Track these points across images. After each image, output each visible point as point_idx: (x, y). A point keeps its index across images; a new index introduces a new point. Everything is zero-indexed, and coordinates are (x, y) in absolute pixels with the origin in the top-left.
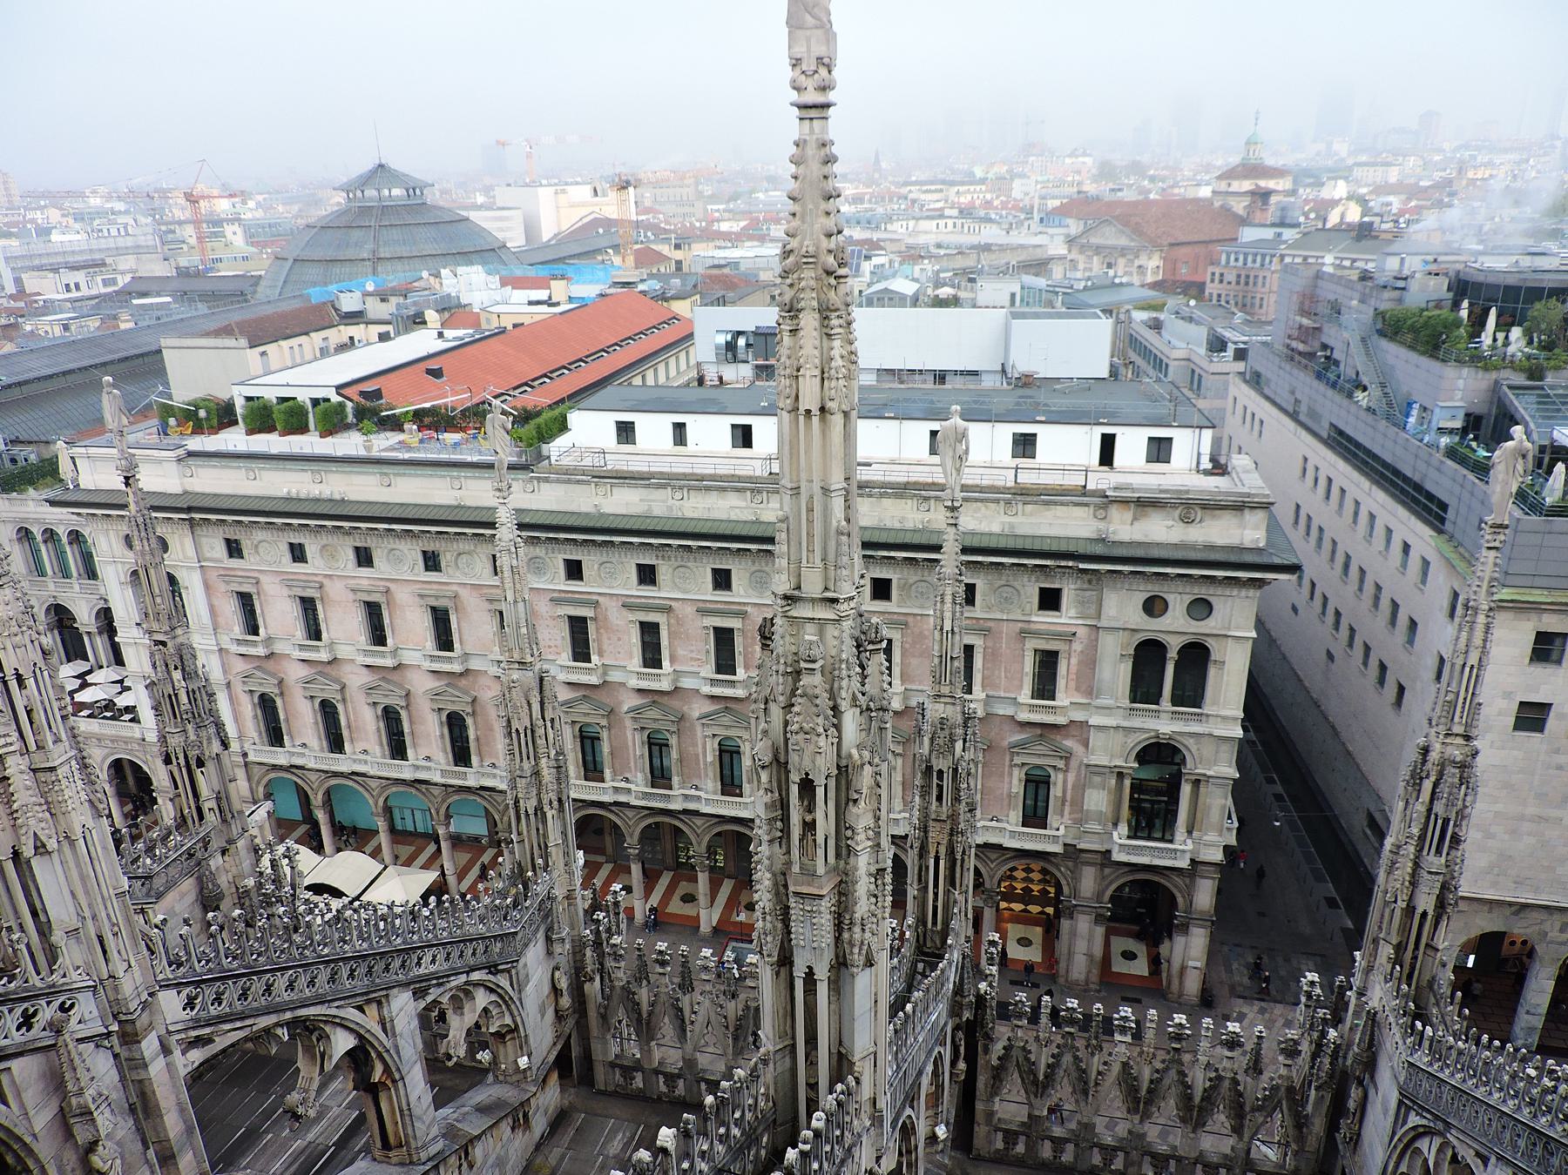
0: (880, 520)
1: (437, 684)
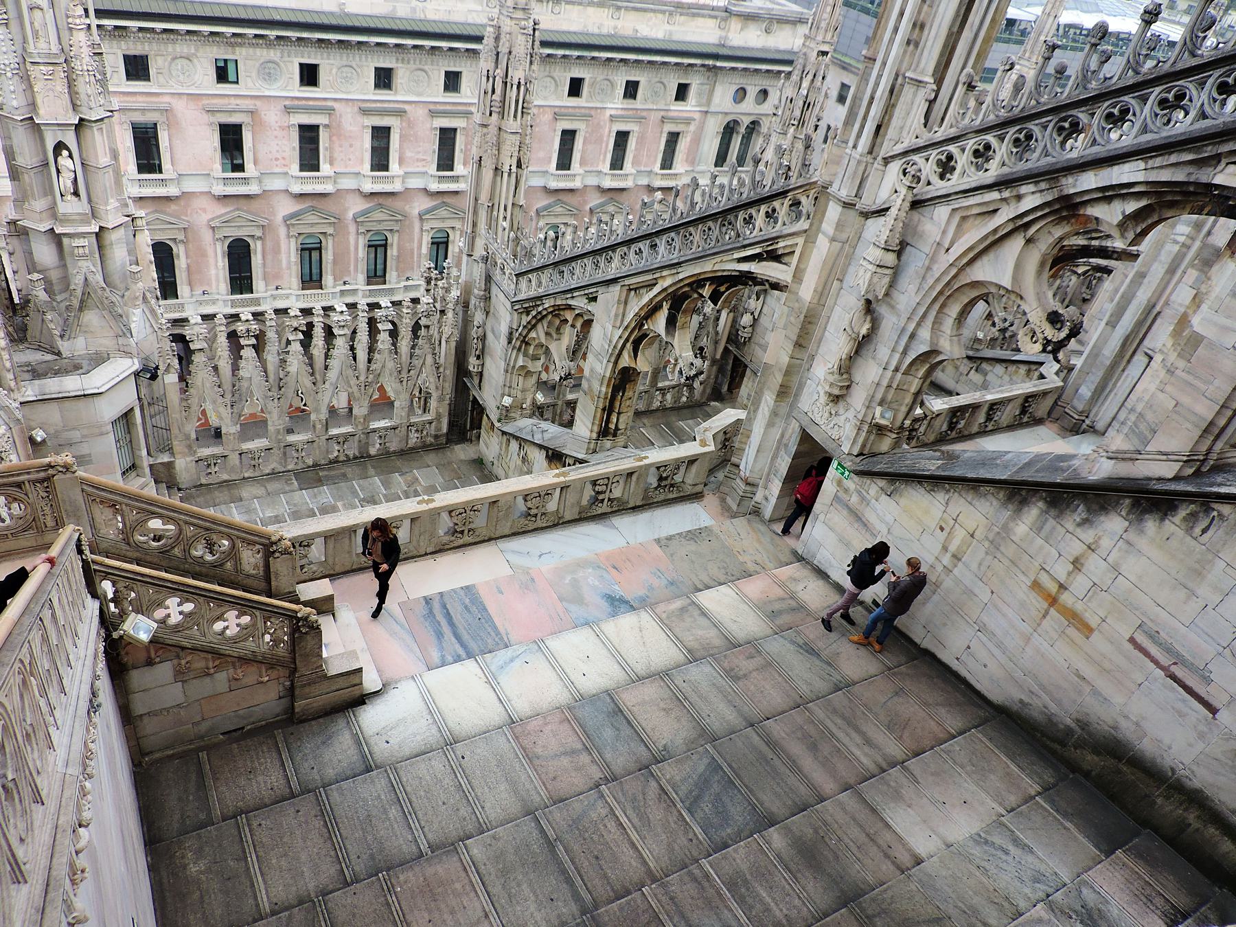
1: (223, 211)
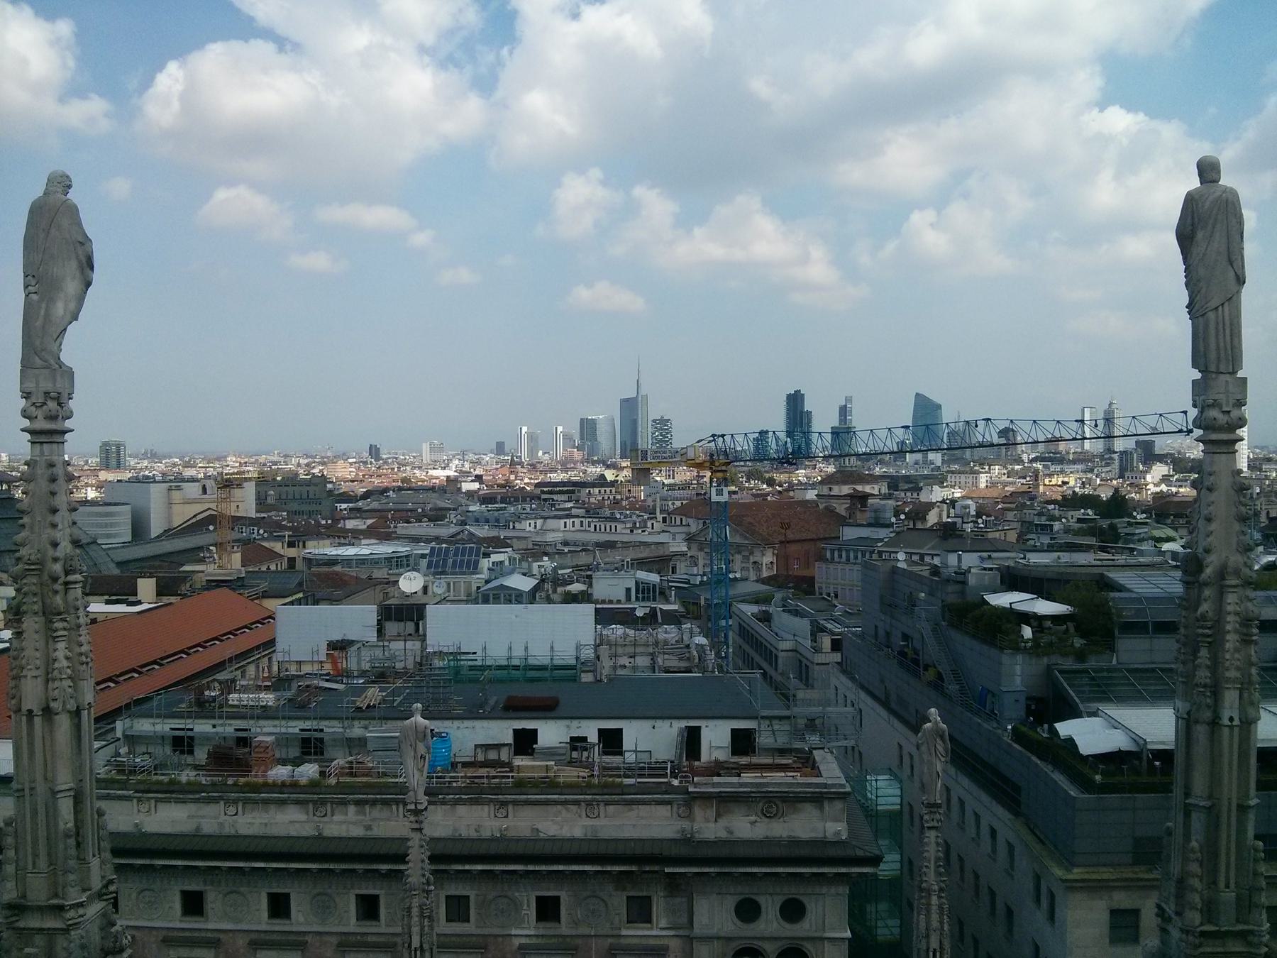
0: (455, 830)
